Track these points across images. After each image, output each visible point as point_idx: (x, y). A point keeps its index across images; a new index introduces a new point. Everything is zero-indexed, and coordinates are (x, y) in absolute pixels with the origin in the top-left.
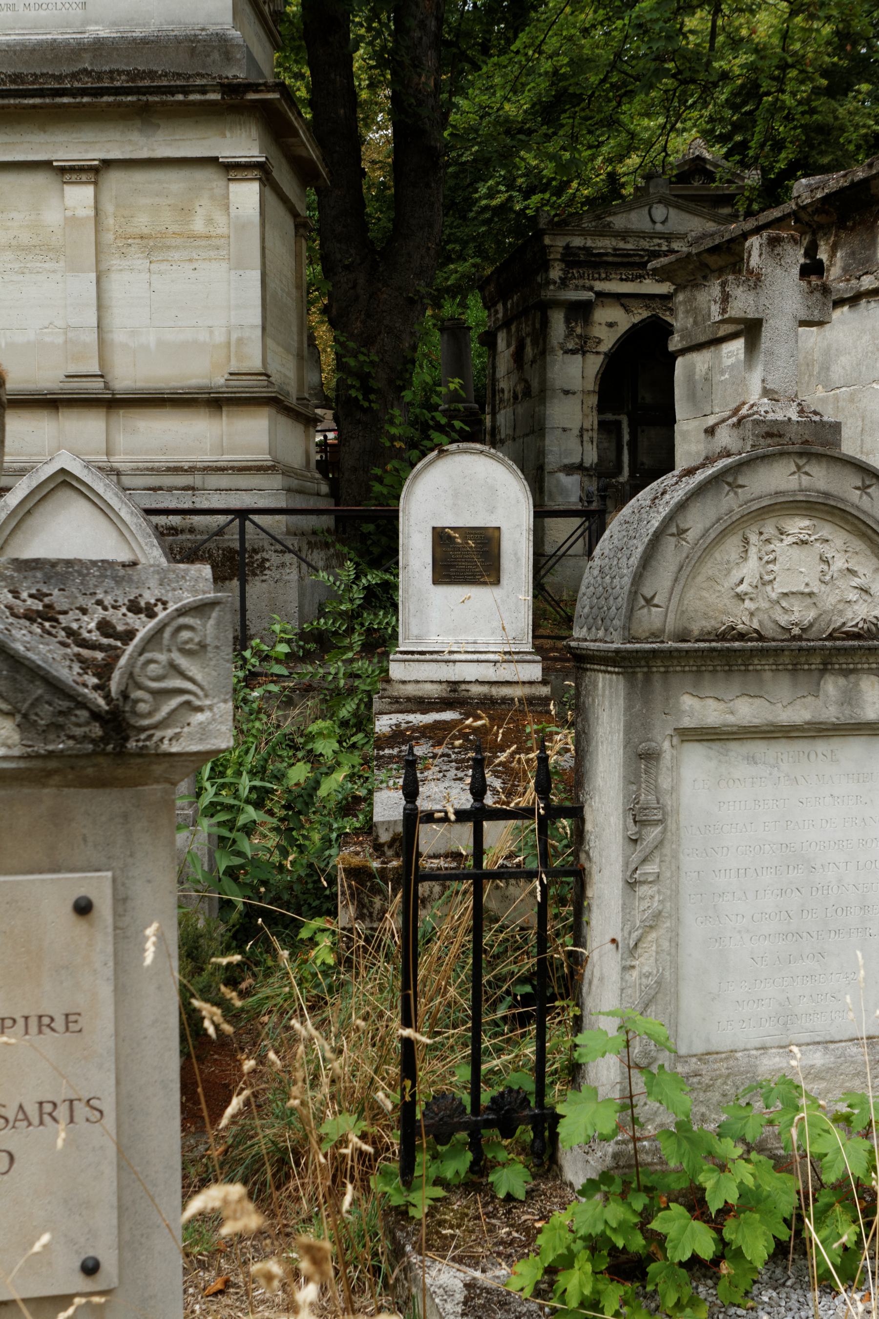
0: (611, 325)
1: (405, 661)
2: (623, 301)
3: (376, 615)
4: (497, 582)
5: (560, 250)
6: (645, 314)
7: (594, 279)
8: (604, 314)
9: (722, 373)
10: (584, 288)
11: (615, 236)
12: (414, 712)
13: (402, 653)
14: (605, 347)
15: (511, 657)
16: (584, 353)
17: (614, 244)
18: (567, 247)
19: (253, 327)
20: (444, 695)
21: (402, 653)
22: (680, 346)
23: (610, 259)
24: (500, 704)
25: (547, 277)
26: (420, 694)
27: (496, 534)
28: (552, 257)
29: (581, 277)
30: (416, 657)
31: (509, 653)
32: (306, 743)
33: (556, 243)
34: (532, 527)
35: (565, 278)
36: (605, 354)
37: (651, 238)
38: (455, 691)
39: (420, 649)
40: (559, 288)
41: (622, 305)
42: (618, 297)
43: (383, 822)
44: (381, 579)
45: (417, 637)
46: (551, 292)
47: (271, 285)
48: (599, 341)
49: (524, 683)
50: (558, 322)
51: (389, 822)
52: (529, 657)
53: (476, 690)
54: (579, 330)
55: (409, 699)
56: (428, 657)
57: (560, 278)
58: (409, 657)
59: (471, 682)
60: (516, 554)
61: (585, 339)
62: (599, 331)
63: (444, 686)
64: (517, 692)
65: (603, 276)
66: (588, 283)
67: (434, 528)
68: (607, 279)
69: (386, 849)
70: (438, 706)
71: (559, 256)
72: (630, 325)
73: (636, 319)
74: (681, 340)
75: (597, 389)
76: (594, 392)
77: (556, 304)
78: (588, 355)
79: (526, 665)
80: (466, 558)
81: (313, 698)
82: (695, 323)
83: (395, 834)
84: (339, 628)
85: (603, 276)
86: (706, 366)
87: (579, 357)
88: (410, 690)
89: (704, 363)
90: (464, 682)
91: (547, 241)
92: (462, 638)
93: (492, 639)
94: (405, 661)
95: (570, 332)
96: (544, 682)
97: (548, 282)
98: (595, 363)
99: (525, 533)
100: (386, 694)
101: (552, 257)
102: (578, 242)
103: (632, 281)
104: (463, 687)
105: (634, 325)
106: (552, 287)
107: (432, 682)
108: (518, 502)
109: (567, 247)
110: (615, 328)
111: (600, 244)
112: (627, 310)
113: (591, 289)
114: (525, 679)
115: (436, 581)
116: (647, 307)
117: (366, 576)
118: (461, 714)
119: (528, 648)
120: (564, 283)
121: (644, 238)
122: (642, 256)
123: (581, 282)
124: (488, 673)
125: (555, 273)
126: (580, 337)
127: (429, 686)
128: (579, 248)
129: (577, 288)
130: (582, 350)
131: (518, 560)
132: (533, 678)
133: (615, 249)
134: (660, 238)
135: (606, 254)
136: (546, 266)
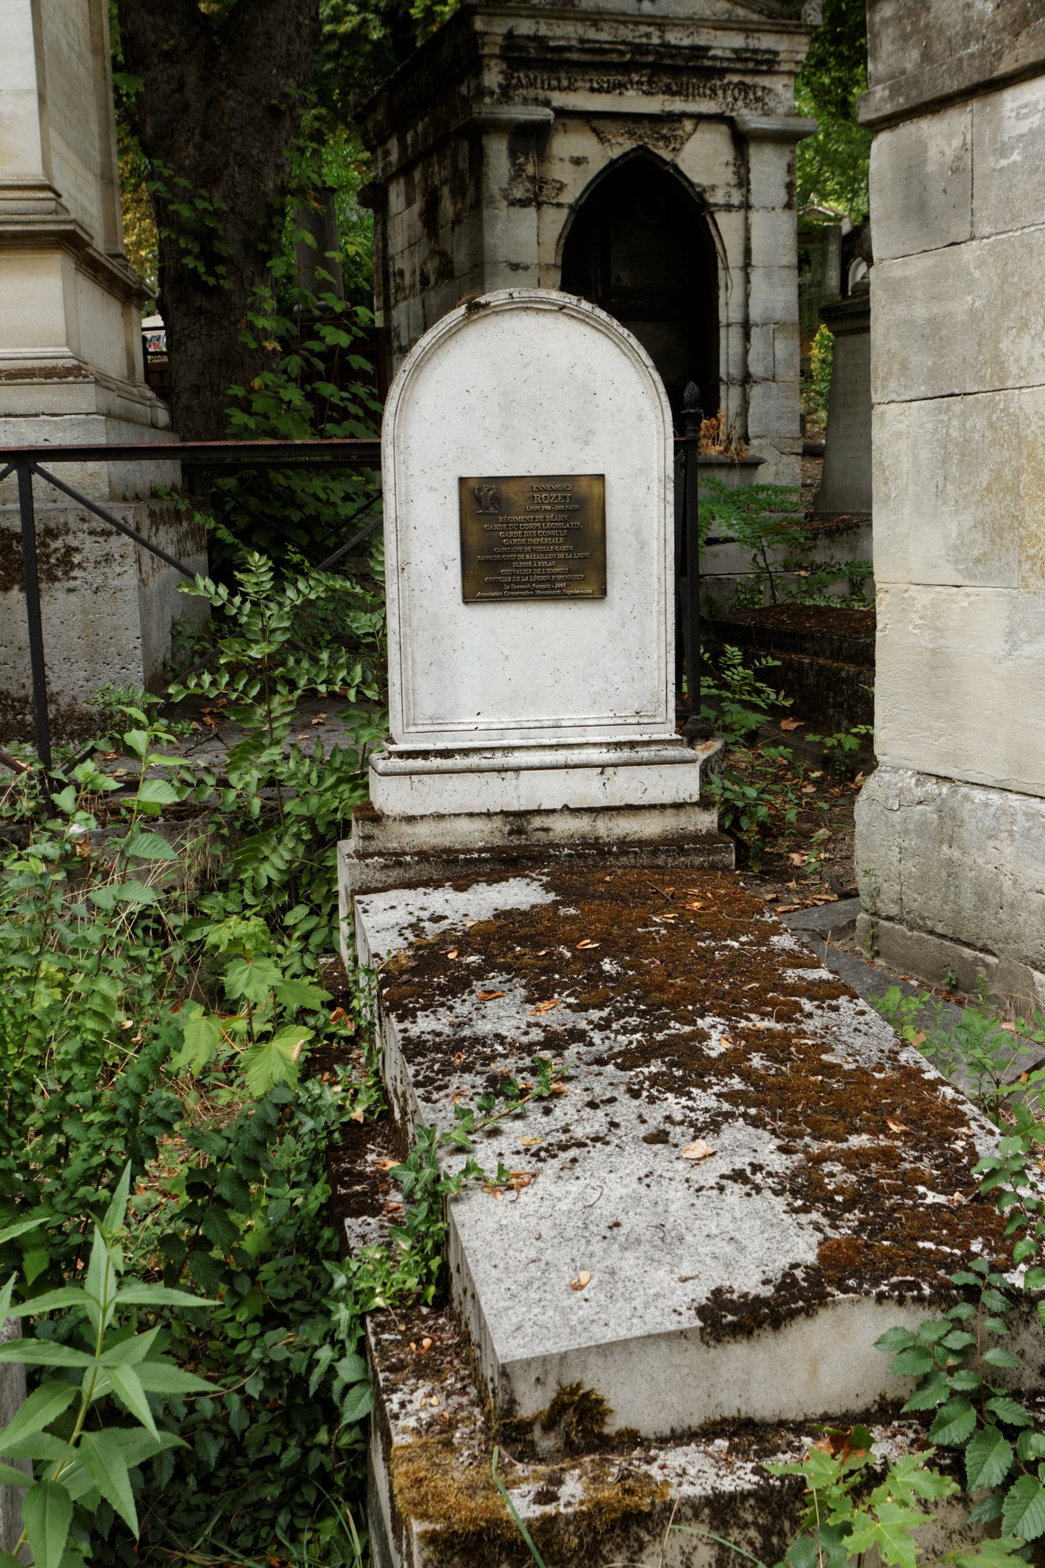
0: (577, 161)
1: (411, 773)
2: (595, 123)
3: (315, 661)
4: (601, 593)
5: (499, 40)
6: (629, 145)
7: (552, 89)
8: (569, 144)
9: (1003, 151)
10: (536, 101)
11: (582, 20)
12: (438, 885)
13: (401, 755)
14: (569, 197)
15: (632, 752)
16: (539, 206)
17: (581, 31)
18: (510, 36)
19: (18, 93)
20: (498, 841)
21: (401, 755)
22: (888, 109)
23: (575, 56)
24: (616, 856)
25: (479, 84)
26: (446, 842)
27: (596, 490)
28: (486, 51)
29: (532, 84)
30: (436, 762)
31: (632, 745)
32: (188, 929)
33: (493, 29)
34: (671, 474)
35: (508, 86)
36: (571, 207)
37: (636, 24)
38: (519, 832)
39: (440, 746)
40: (499, 102)
41: (594, 130)
42: (588, 118)
43: (528, 1363)
44: (328, 589)
45: (434, 720)
46: (486, 108)
47: (52, 27)
48: (561, 187)
49: (663, 807)
50: (498, 154)
51: (545, 1360)
52: (672, 752)
53: (564, 827)
54: (530, 169)
55: (423, 855)
56: (459, 762)
57: (500, 86)
58: (419, 763)
59: (553, 811)
60: (637, 533)
61: (539, 182)
62: (560, 171)
63: (497, 822)
64: (650, 827)
65: (565, 83)
66: (542, 95)
67: (462, 481)
68: (571, 88)
69: (537, 1432)
70: (487, 868)
71: (497, 51)
72: (606, 162)
73: (616, 153)
74: (891, 98)
75: (559, 262)
76: (555, 266)
77: (496, 126)
78: (545, 208)
79: (666, 769)
80: (532, 542)
81: (195, 832)
82: (927, 57)
83: (562, 1391)
84: (245, 692)
85: (565, 83)
86: (957, 143)
87: (532, 211)
88: (425, 835)
89: (949, 137)
90: (539, 812)
91: (479, 25)
92: (530, 716)
93: (592, 717)
94: (411, 773)
95: (518, 171)
96: (705, 803)
97: (481, 92)
98: (555, 222)
99: (656, 487)
100: (373, 846)
101: (486, 51)
102: (525, 27)
103: (608, 92)
104: (537, 822)
105: (612, 162)
106: (487, 100)
107: (471, 815)
108: (640, 419)
109: (510, 36)
110: (584, 166)
111: (559, 32)
112: (602, 140)
113: (547, 103)
114: (666, 799)
115: (469, 598)
116: (631, 134)
117: (294, 583)
118: (547, 887)
119: (668, 731)
120: (506, 94)
121: (625, 23)
122: (622, 53)
123: (531, 93)
124: (589, 789)
125: (493, 78)
126: (532, 179)
127: (464, 826)
128: (528, 38)
129: (525, 101)
130: (535, 200)
131: (643, 545)
132: (682, 796)
133: (582, 41)
134: (649, 25)
135: (569, 49)
136: (476, 66)
